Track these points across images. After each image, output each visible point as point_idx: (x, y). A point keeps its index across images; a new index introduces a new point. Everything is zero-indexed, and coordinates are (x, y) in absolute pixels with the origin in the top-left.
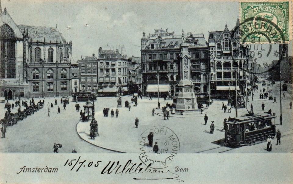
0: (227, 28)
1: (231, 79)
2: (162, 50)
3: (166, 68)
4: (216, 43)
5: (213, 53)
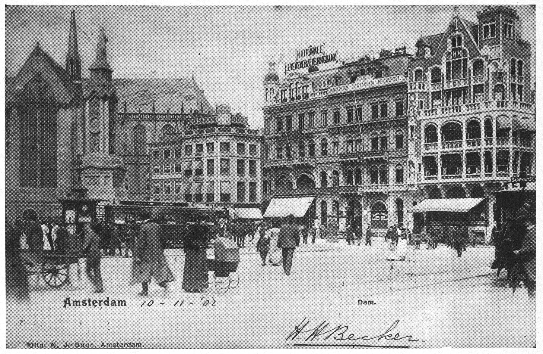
1: (461, 177)
2: (290, 106)
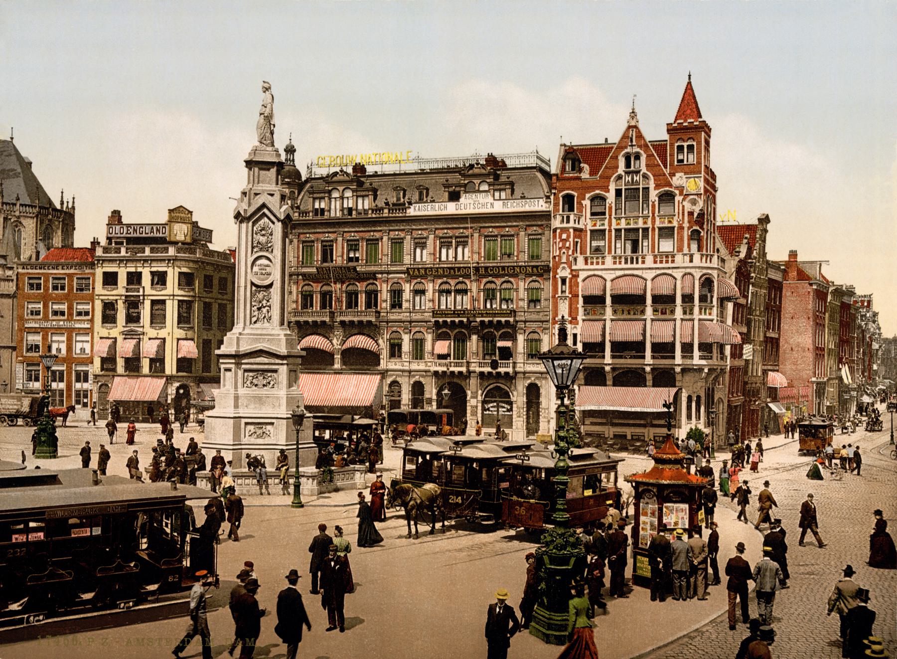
0: (636, 127)
3: (372, 298)
4: (588, 196)
5: (571, 240)
